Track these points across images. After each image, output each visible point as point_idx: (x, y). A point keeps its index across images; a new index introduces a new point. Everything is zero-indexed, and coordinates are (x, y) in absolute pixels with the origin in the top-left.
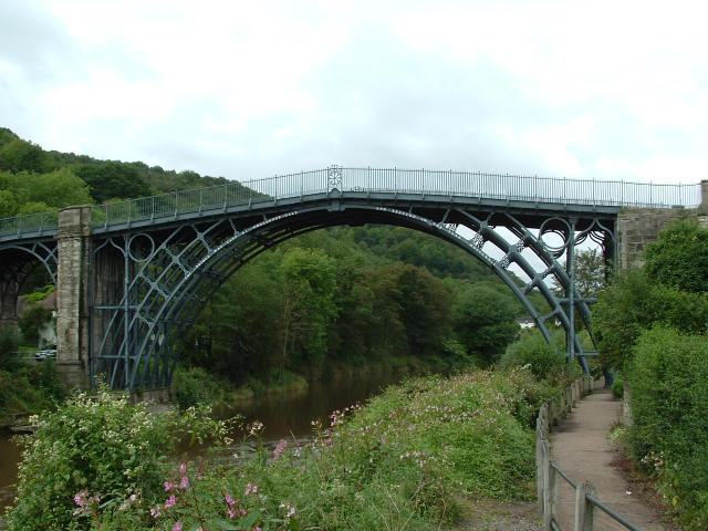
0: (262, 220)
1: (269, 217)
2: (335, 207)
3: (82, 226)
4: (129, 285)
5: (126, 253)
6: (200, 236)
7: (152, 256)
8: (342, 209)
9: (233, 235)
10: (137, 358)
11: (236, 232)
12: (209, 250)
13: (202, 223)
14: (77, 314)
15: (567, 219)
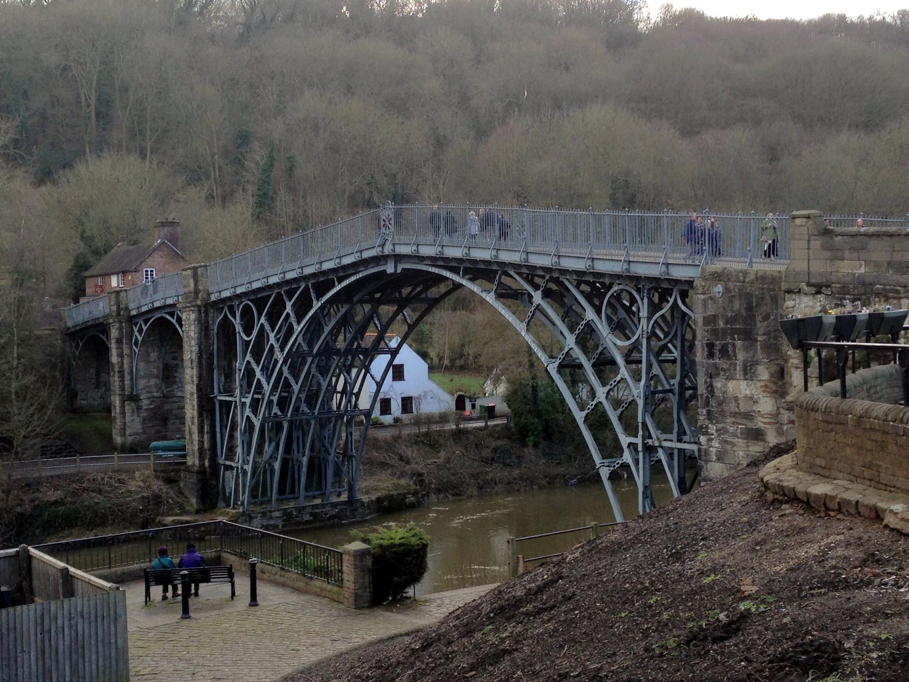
0: (333, 286)
1: (341, 280)
2: (390, 269)
3: (196, 292)
4: (240, 370)
5: (238, 328)
6: (289, 308)
7: (255, 333)
8: (399, 271)
9: (311, 307)
10: (249, 468)
11: (315, 302)
12: (295, 327)
13: (289, 287)
14: (196, 407)
15: (639, 290)
